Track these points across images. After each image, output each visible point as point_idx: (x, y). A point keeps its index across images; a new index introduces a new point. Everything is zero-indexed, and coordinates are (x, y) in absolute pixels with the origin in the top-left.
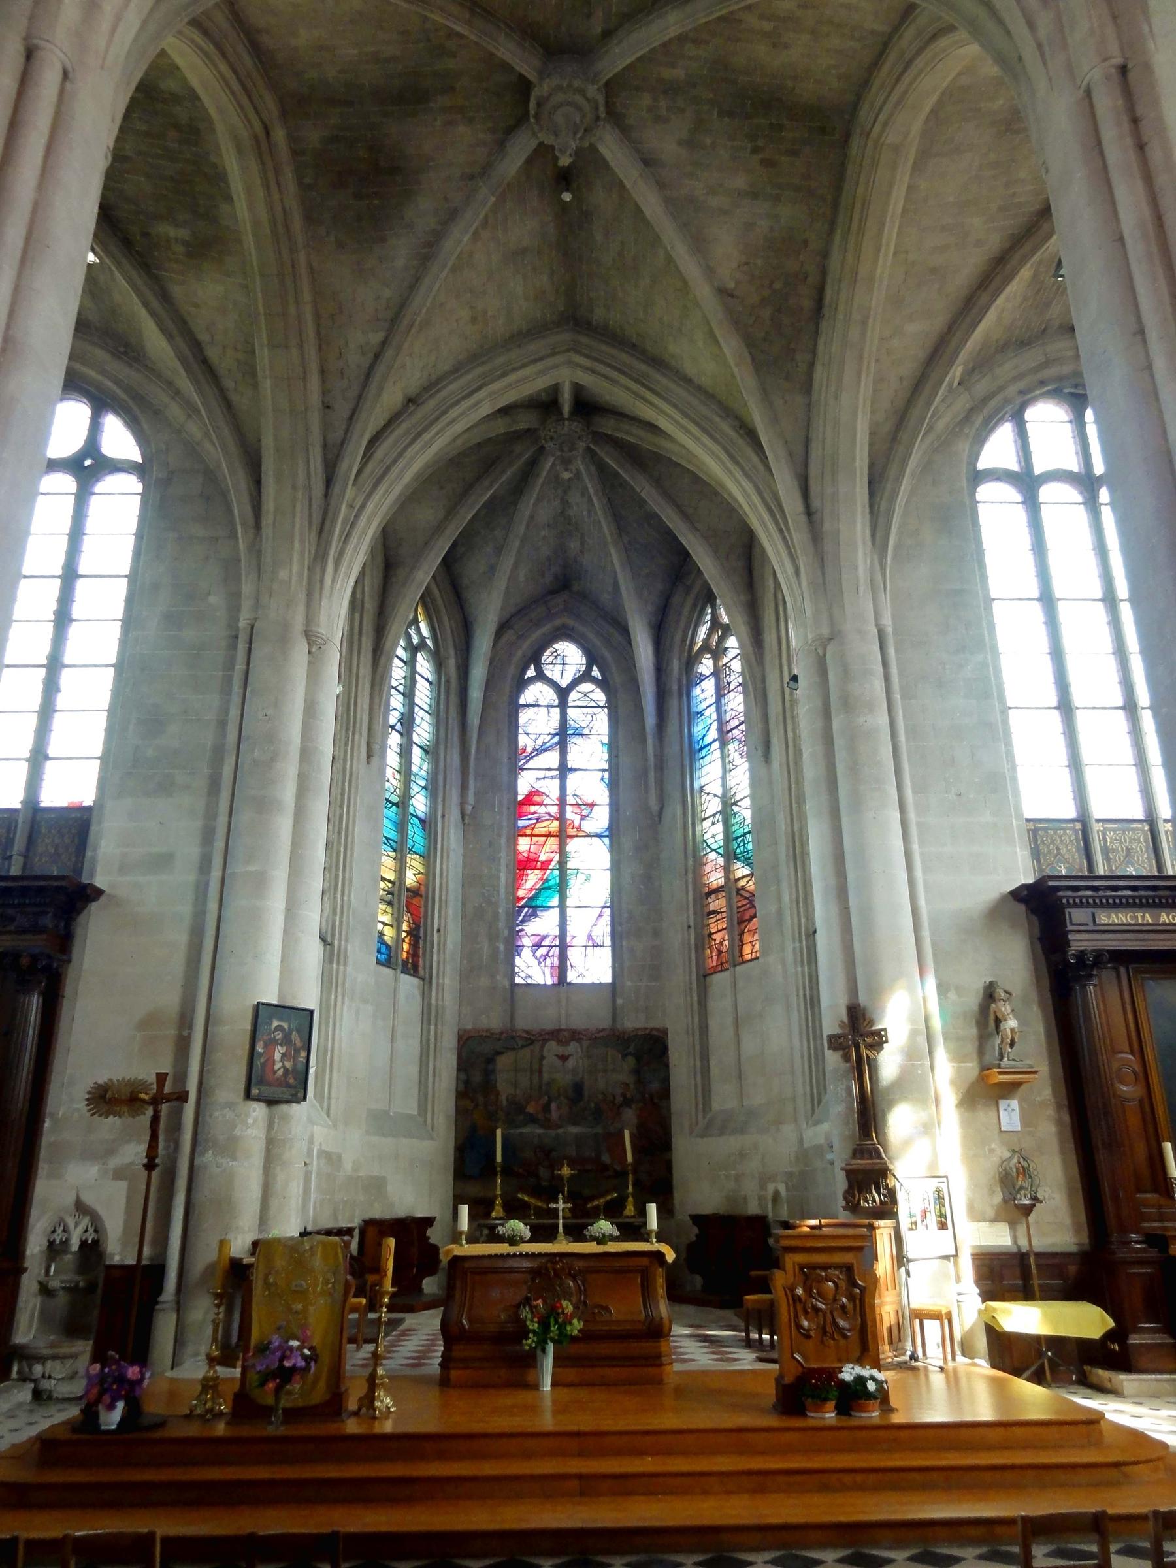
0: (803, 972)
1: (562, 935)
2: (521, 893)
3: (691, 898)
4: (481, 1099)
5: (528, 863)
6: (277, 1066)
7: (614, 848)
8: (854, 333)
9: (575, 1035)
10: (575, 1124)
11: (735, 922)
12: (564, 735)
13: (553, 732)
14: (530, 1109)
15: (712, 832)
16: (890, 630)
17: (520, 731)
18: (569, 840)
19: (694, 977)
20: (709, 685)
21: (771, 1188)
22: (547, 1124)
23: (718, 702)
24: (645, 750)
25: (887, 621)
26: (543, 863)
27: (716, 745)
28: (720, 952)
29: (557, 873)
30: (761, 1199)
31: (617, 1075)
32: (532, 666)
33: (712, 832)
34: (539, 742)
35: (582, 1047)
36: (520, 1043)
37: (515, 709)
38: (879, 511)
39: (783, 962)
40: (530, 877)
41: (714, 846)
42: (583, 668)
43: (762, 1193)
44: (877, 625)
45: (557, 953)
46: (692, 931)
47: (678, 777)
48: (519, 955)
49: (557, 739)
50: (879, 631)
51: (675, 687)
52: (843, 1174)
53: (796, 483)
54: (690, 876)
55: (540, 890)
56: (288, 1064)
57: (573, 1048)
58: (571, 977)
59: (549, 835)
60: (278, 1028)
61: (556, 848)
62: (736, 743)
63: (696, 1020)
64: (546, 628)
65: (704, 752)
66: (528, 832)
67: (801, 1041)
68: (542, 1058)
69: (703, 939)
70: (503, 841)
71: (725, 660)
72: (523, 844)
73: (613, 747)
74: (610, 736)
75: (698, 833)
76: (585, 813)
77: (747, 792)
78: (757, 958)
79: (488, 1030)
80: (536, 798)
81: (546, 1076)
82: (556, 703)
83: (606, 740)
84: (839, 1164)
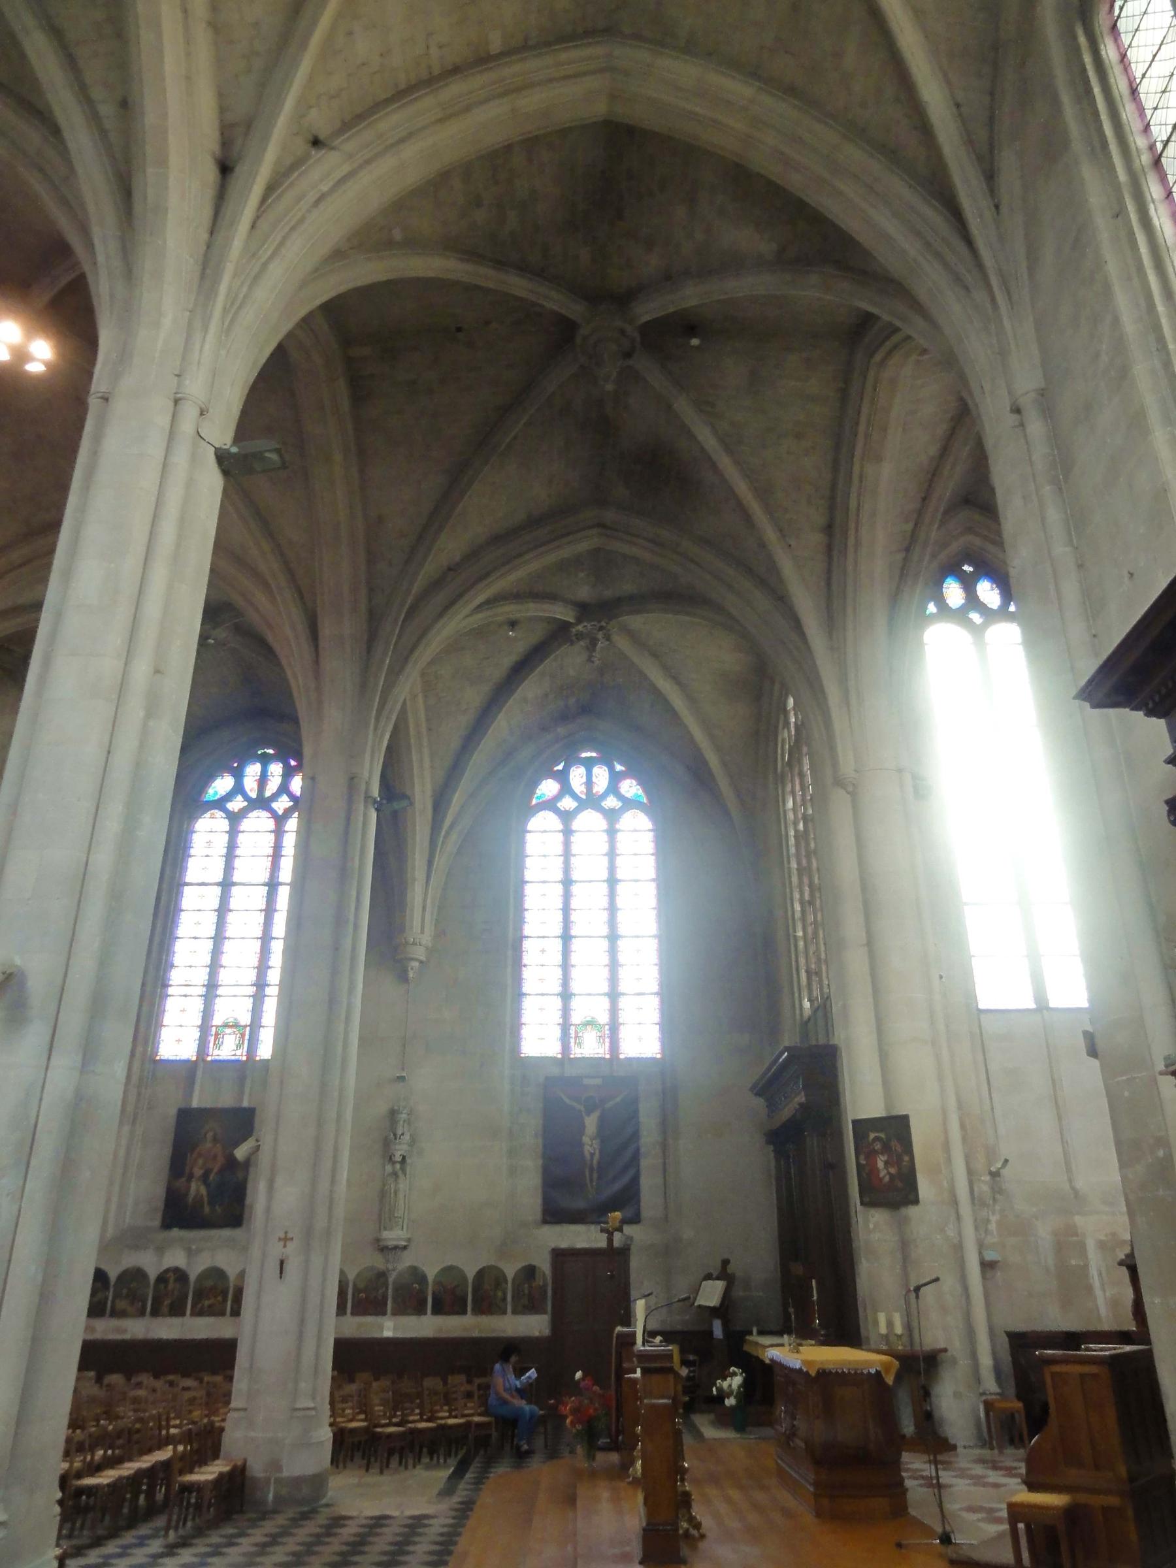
6: (882, 1174)
56: (892, 1170)
60: (877, 1139)
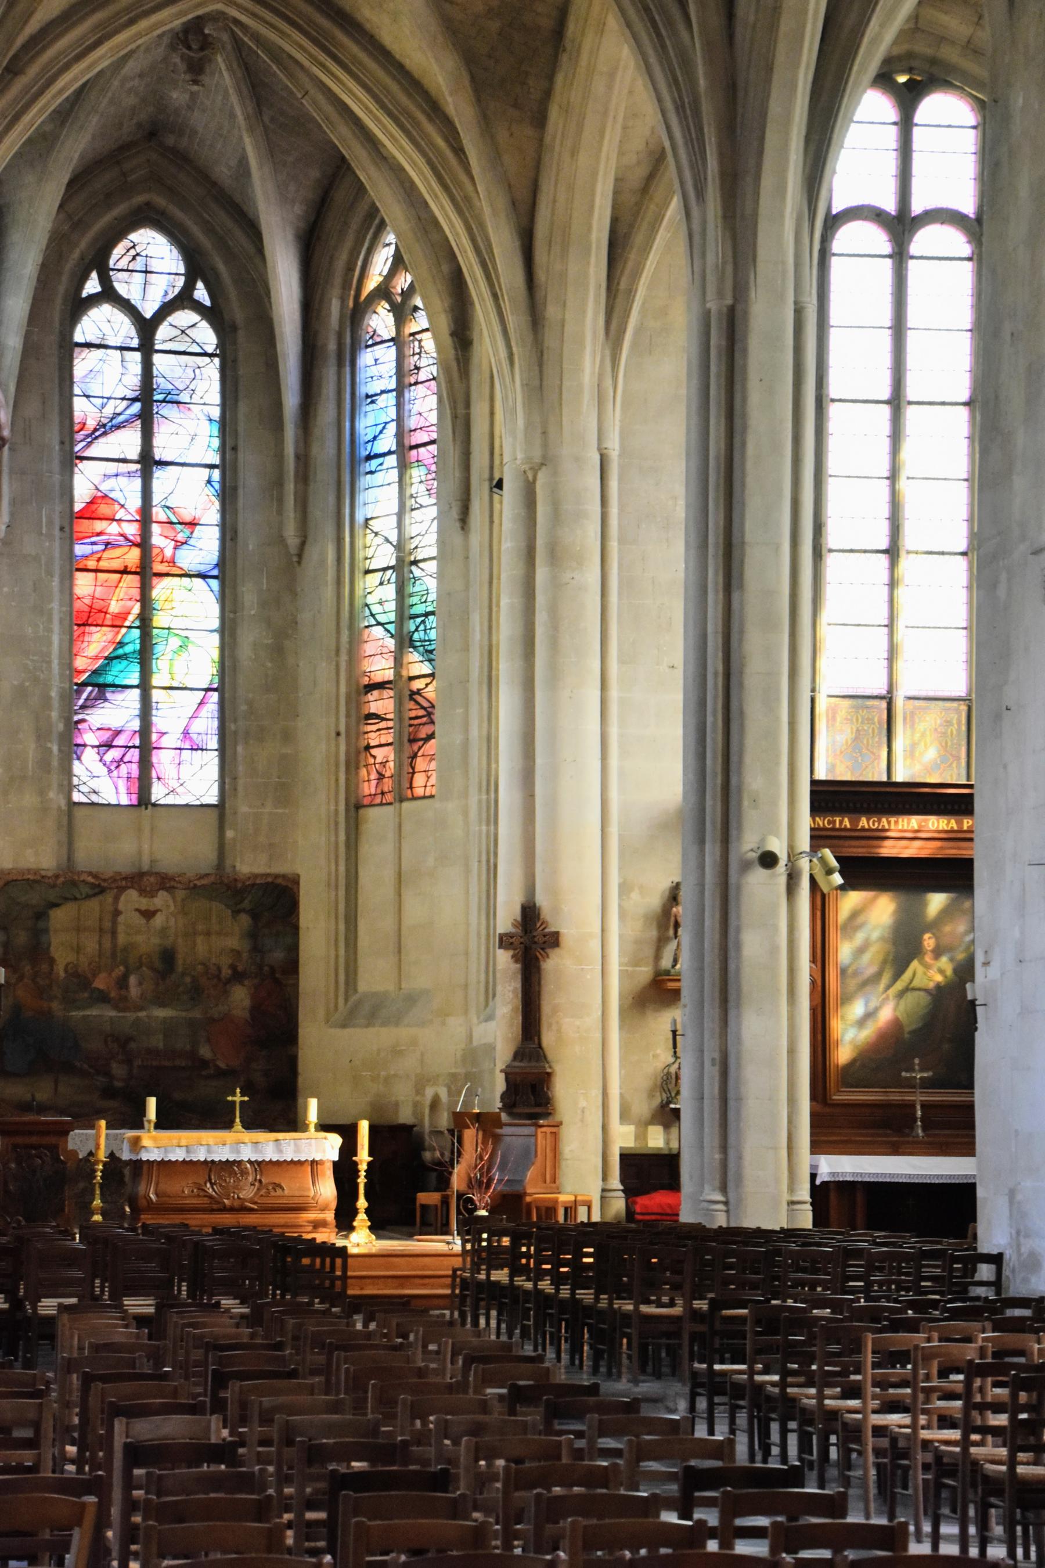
0: (488, 832)
1: (145, 731)
2: (80, 663)
3: (343, 689)
4: (27, 969)
5: (90, 617)
7: (228, 601)
8: (599, 86)
9: (165, 882)
10: (163, 1005)
11: (406, 739)
12: (148, 401)
13: (130, 394)
14: (100, 983)
15: (380, 596)
16: (614, 454)
17: (77, 390)
18: (155, 580)
19: (342, 807)
20: (388, 354)
21: (429, 1093)
22: (122, 1003)
23: (400, 390)
24: (280, 441)
25: (613, 445)
26: (116, 616)
27: (392, 460)
28: (381, 777)
29: (136, 633)
30: (416, 1105)
31: (224, 940)
32: (94, 275)
33: (380, 596)
34: (109, 411)
35: (174, 898)
36: (85, 890)
37: (68, 349)
38: (617, 290)
39: (466, 813)
40: (96, 637)
41: (382, 619)
42: (180, 282)
43: (418, 1098)
44: (599, 449)
45: (136, 758)
46: (342, 739)
47: (332, 499)
48: (79, 758)
49: (137, 407)
50: (602, 456)
51: (332, 346)
52: (502, 1076)
53: (517, 244)
54: (344, 657)
55: (110, 659)
57: (161, 899)
58: (158, 793)
59: (125, 571)
61: (136, 593)
62: (423, 470)
63: (342, 868)
64: (120, 209)
65: (374, 464)
66: (91, 564)
67: (479, 918)
68: (117, 913)
69: (358, 753)
70: (56, 583)
71: (413, 327)
72: (84, 585)
73: (227, 426)
74: (223, 405)
75: (359, 592)
76: (181, 537)
77: (433, 552)
78: (432, 796)
79: (36, 872)
80: (103, 509)
81: (122, 939)
82: (135, 343)
83: (216, 413)
84: (500, 1065)
